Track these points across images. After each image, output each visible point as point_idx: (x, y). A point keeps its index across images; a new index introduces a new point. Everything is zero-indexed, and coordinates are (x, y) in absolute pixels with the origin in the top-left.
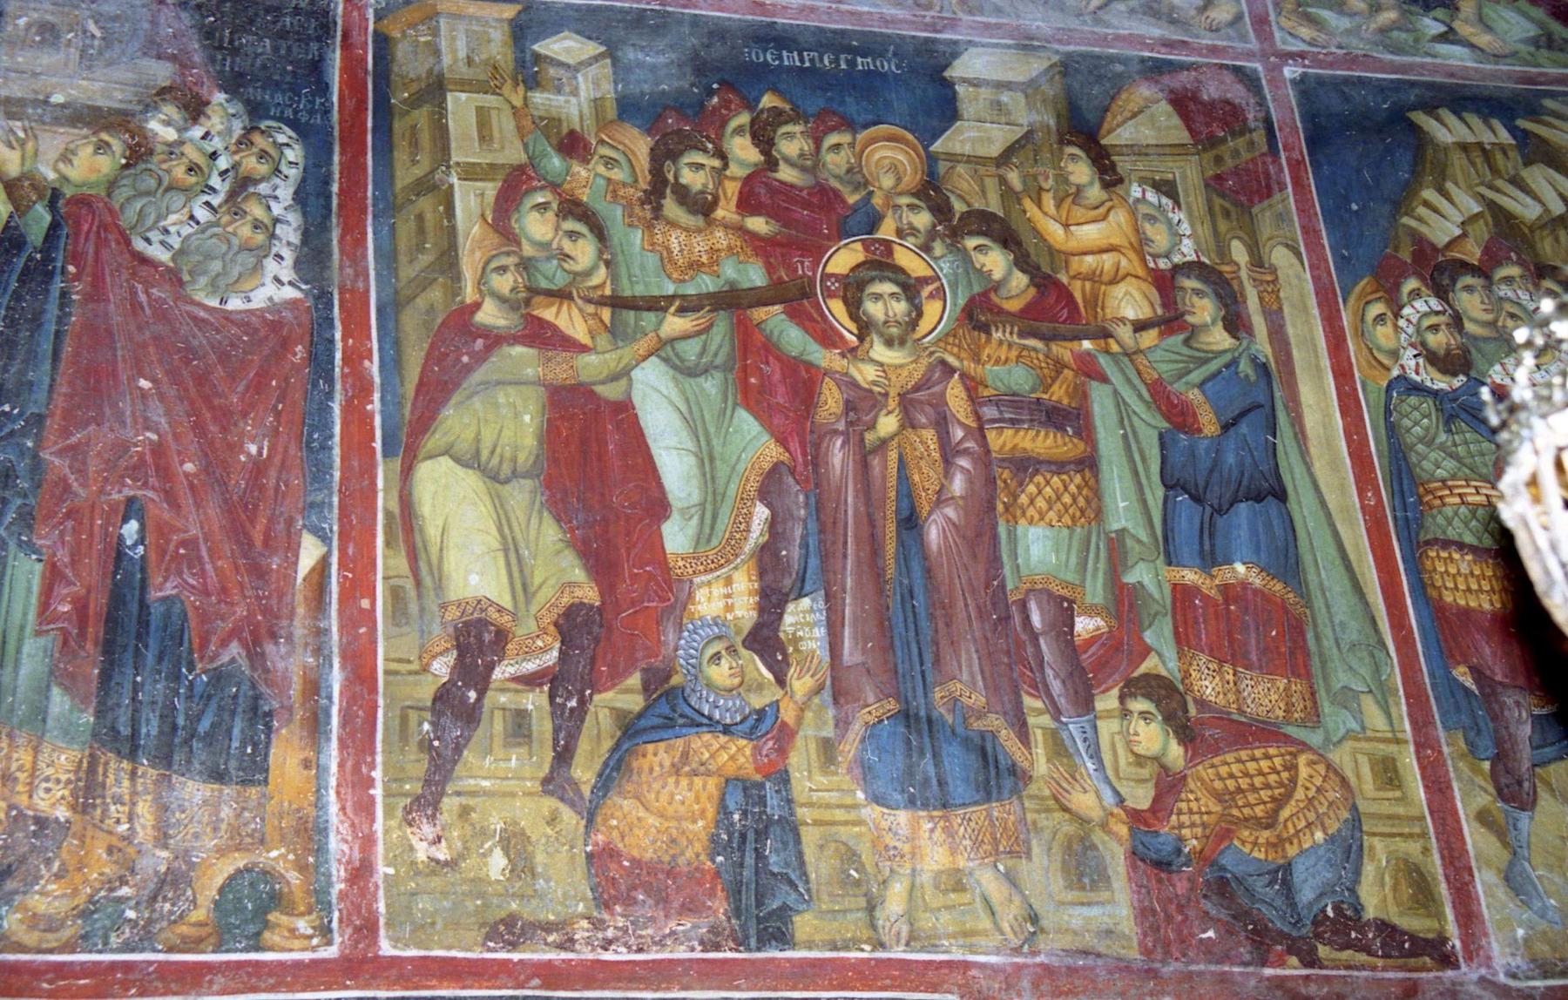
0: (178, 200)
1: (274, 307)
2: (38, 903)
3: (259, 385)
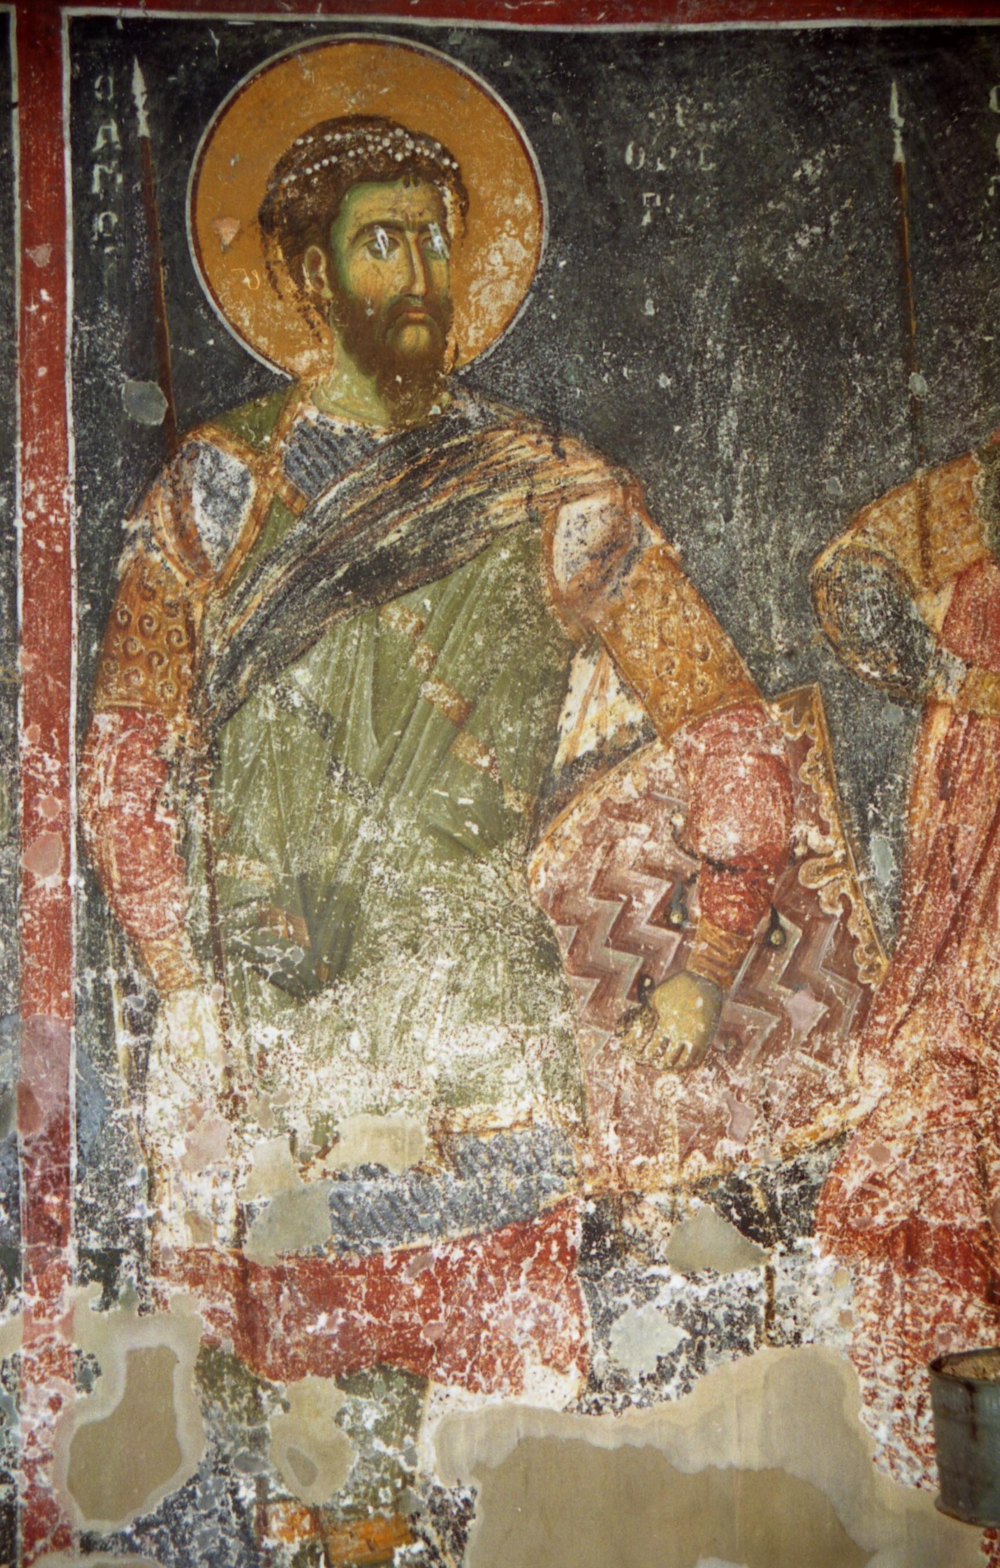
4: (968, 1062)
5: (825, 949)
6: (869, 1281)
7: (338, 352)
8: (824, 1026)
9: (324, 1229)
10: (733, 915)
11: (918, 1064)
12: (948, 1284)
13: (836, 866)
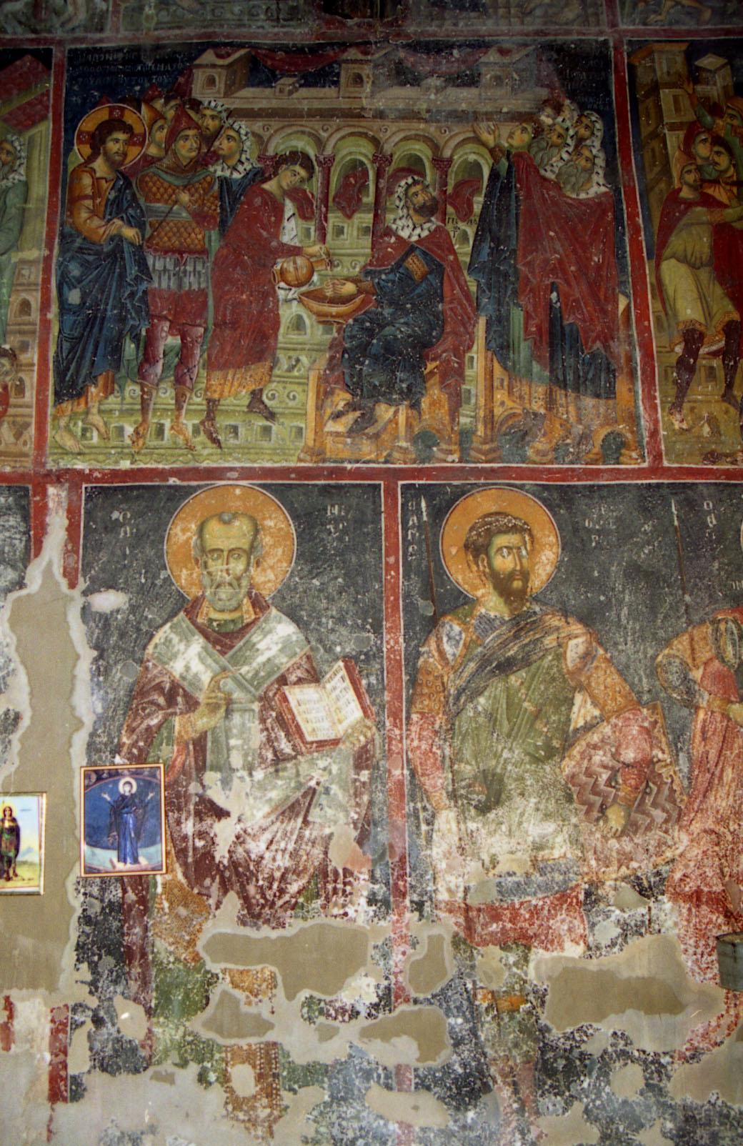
0: (556, 151)
1: (598, 196)
2: (539, 446)
3: (596, 232)
7: (491, 590)
8: (666, 821)
9: (494, 895)
10: (633, 782)
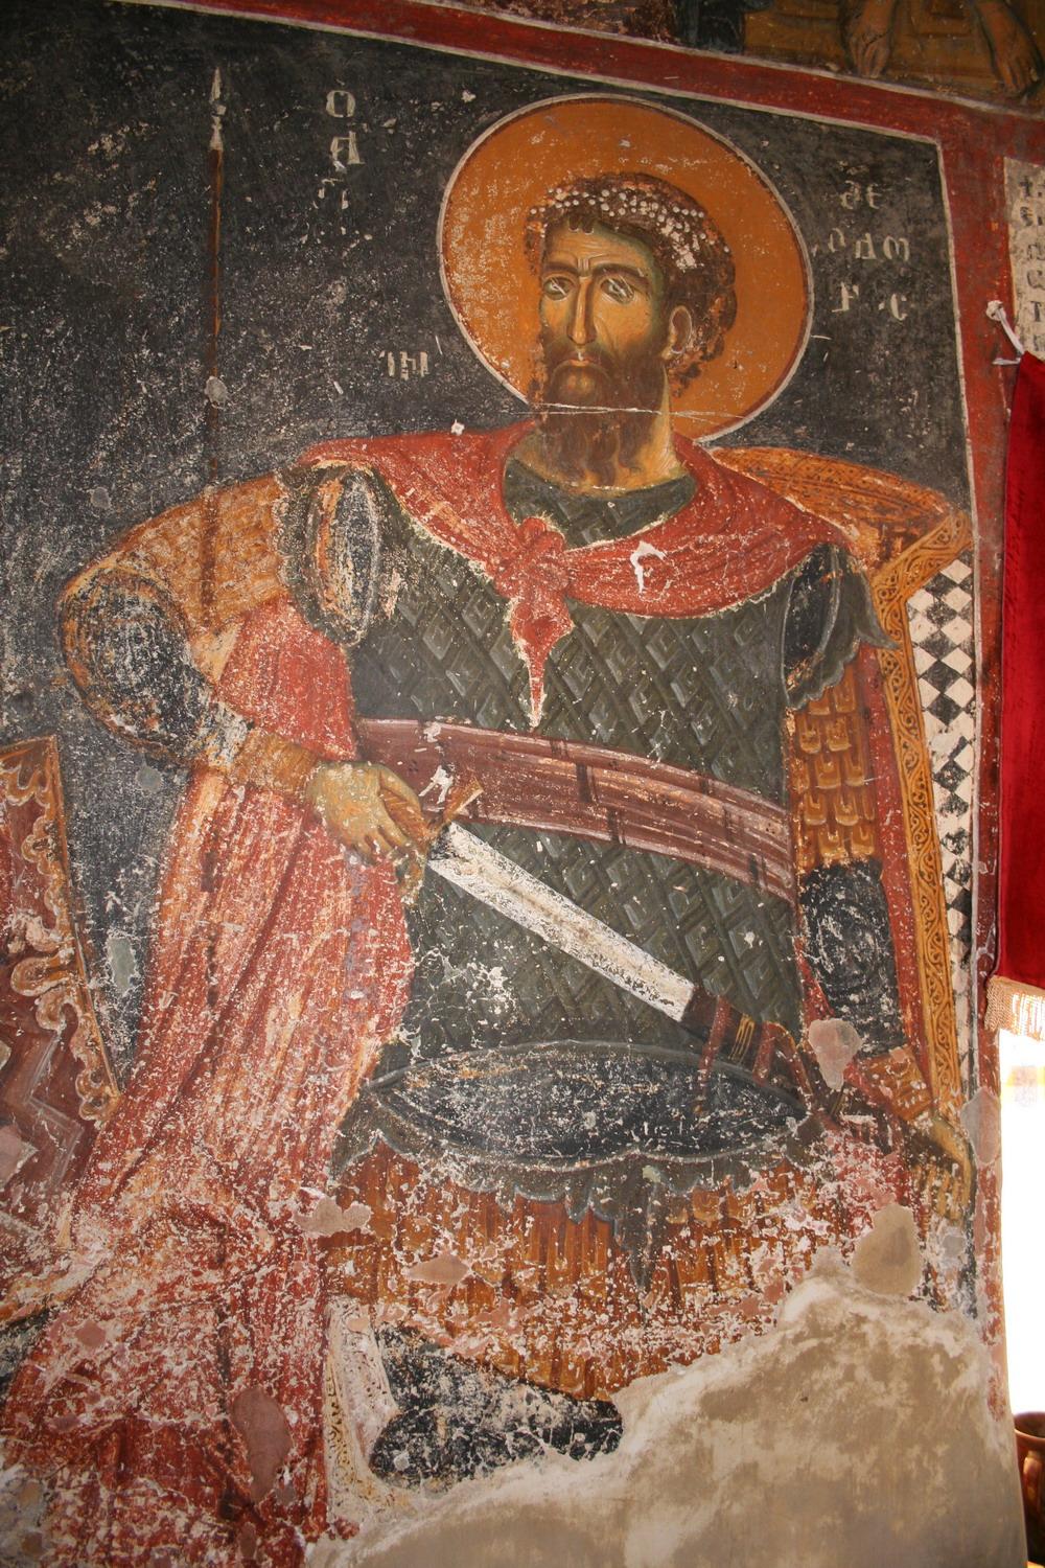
4: (214, 1223)
5: (40, 1074)
6: (67, 1495)
8: (30, 1174)
11: (150, 1223)
12: (170, 1497)
13: (61, 968)
